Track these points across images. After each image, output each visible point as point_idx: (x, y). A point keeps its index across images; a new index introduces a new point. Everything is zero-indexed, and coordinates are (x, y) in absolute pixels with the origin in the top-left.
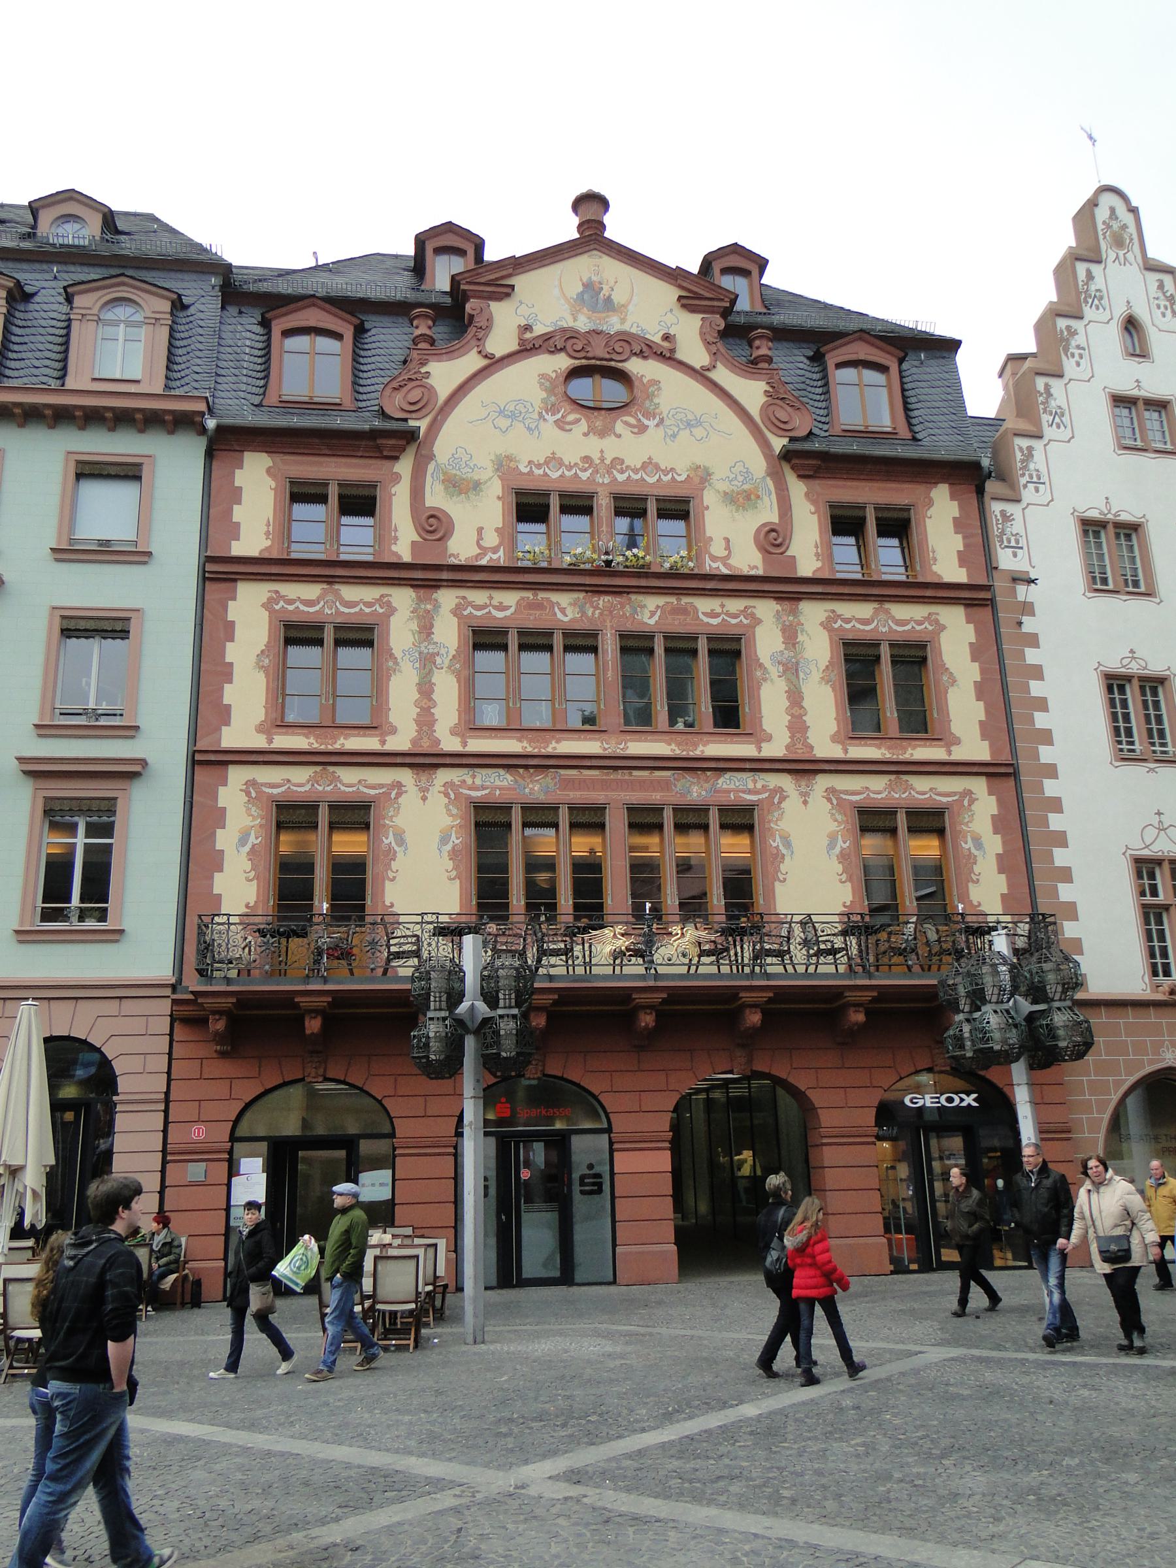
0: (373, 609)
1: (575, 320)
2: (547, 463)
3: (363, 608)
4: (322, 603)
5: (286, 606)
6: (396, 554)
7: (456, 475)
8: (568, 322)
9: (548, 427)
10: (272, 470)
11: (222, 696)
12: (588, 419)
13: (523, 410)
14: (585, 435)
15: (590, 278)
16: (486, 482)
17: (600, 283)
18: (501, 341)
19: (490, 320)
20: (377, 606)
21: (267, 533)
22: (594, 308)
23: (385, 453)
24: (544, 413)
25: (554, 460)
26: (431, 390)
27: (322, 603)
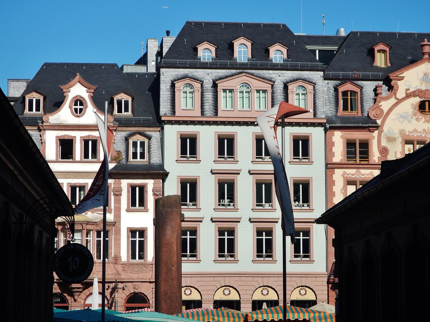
0: (369, 176)
1: (421, 86)
2: (413, 131)
3: (366, 176)
4: (356, 175)
5: (347, 176)
6: (374, 160)
7: (389, 136)
8: (419, 87)
9: (414, 121)
10: (342, 136)
11: (333, 201)
12: (425, 117)
13: (407, 115)
14: (424, 122)
15: (426, 71)
16: (397, 138)
17: (429, 73)
18: (401, 94)
19: (398, 87)
20: (370, 175)
21: (342, 155)
22: (427, 82)
23: (371, 131)
24: (413, 116)
25: (415, 131)
26: (382, 111)
27: (356, 175)
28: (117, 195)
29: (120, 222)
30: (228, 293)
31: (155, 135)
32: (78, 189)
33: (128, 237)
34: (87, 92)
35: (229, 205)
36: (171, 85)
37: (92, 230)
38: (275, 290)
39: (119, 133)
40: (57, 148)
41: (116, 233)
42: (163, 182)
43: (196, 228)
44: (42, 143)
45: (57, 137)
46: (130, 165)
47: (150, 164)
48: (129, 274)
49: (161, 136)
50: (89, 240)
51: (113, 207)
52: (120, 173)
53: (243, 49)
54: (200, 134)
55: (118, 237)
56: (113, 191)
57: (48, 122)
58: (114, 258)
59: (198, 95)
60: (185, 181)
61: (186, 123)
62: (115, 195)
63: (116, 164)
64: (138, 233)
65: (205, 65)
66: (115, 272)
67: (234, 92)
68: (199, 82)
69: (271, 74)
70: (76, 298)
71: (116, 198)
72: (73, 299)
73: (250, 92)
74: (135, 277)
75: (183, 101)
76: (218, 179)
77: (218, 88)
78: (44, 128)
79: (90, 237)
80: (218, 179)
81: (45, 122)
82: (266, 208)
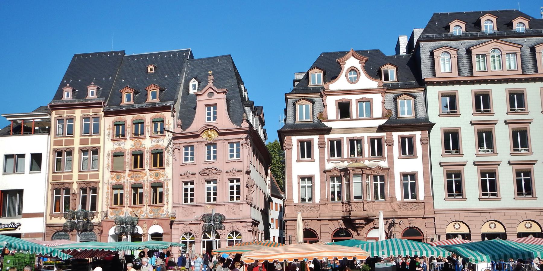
28: (390, 145)
29: (393, 168)
30: (530, 226)
31: (420, 95)
32: (355, 142)
33: (401, 180)
34: (360, 63)
35: (488, 151)
36: (429, 55)
37: (370, 175)
38: (536, 223)
39: (388, 95)
40: (337, 109)
41: (391, 177)
42: (429, 133)
43: (460, 171)
44: (324, 106)
45: (336, 100)
46: (399, 120)
47: (417, 119)
48: (404, 211)
49: (424, 96)
50: (368, 183)
51: (386, 156)
52: (392, 126)
53: (489, 23)
54: (459, 92)
55: (392, 180)
56: (386, 142)
57: (328, 89)
58: (390, 198)
59: (455, 60)
60: (448, 132)
61: (445, 83)
62: (388, 145)
63: (387, 120)
64: (409, 176)
65: (458, 37)
66: (391, 209)
67: (486, 56)
68: (455, 49)
69: (517, 41)
70: (359, 232)
71: (388, 148)
72: (356, 233)
73: (500, 56)
74: (410, 213)
75: (442, 67)
76: (477, 129)
77: (472, 53)
78: (326, 94)
79: (368, 181)
80: (477, 129)
81: (326, 89)
82: (522, 152)
